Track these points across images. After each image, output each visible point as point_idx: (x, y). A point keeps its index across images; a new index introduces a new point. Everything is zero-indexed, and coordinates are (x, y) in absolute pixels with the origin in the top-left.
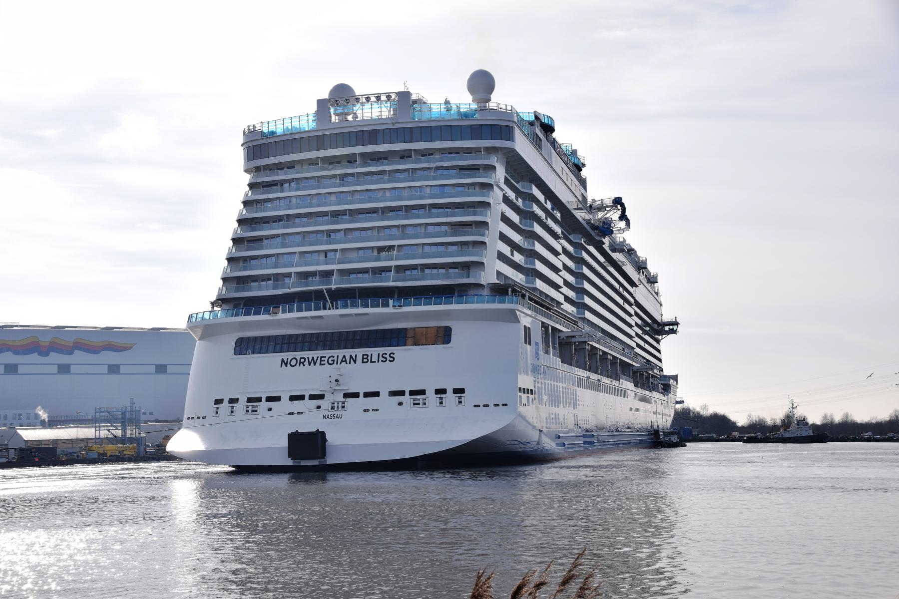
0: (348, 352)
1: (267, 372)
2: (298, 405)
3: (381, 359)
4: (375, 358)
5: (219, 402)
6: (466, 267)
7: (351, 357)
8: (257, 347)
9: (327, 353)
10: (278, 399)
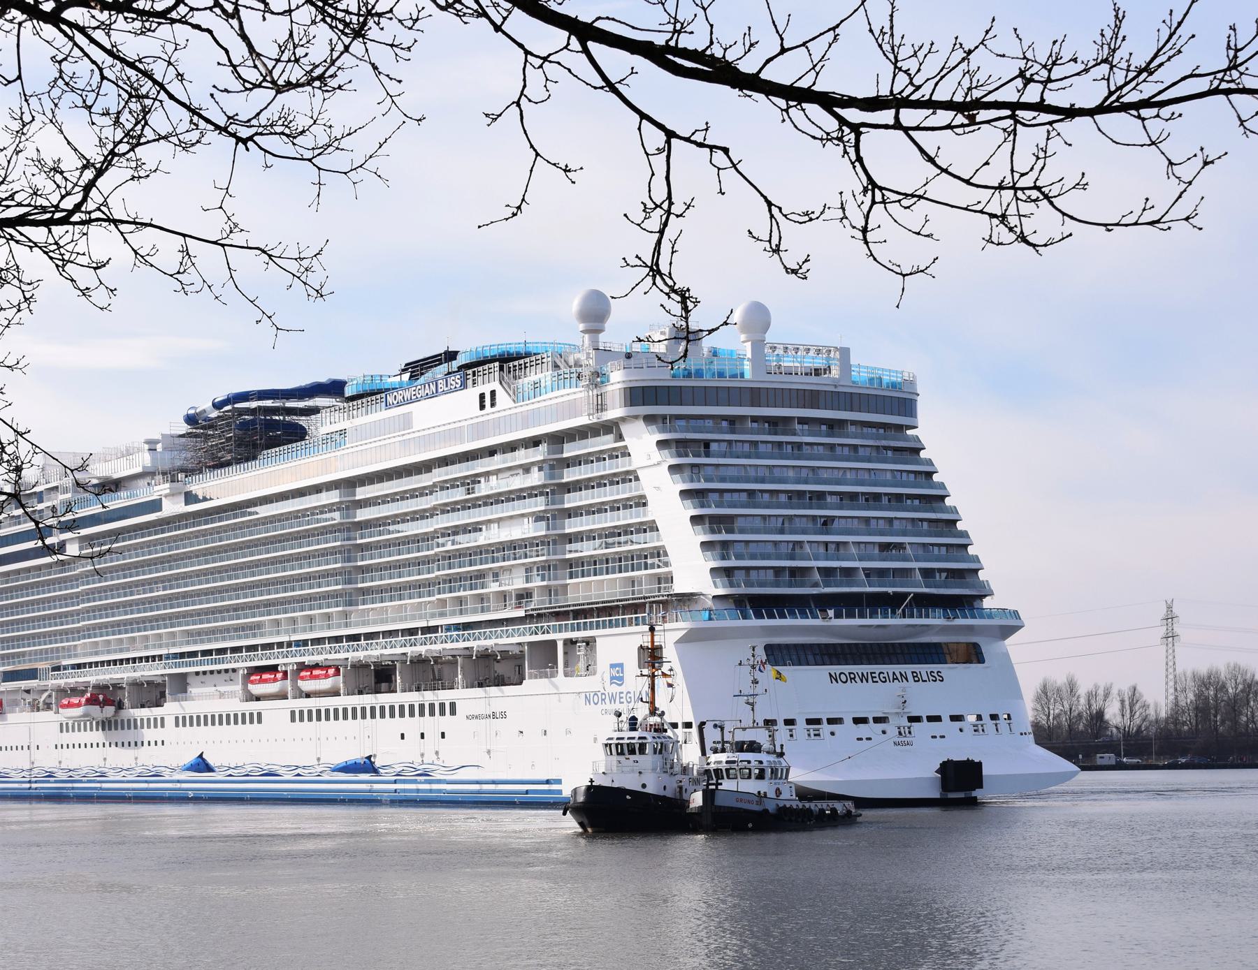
1: (810, 687)
4: (925, 678)
6: (953, 573)
9: (877, 668)
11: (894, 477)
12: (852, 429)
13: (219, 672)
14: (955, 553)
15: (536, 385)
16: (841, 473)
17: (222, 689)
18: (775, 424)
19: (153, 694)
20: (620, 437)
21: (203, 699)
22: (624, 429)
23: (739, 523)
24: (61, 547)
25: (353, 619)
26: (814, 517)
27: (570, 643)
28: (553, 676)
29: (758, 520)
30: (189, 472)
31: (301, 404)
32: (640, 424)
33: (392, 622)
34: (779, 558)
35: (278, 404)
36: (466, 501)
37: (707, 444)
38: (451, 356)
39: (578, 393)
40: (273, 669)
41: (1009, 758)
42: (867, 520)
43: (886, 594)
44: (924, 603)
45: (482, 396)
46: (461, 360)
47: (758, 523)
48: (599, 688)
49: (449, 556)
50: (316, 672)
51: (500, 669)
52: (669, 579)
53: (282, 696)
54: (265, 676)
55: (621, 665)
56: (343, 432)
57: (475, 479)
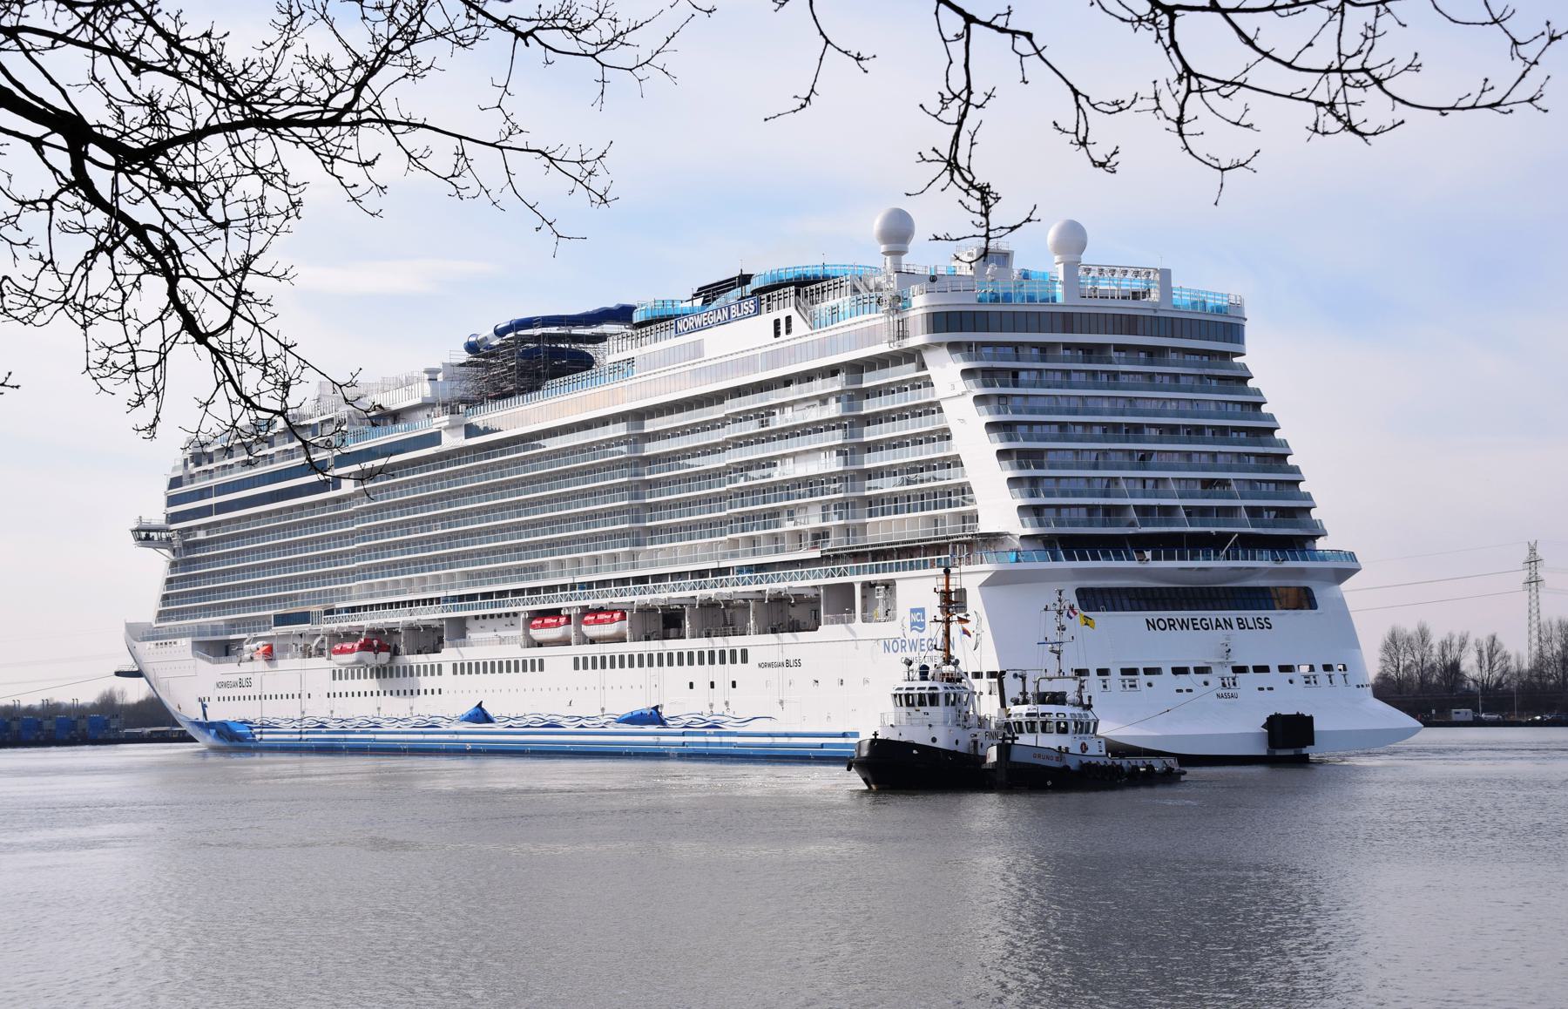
1: (1124, 635)
6: (1281, 512)
11: (1219, 408)
12: (1173, 356)
13: (500, 616)
14: (1285, 490)
15: (834, 311)
16: (1162, 404)
17: (502, 634)
18: (1090, 351)
19: (430, 639)
20: (923, 366)
21: (483, 645)
22: (928, 357)
23: (1049, 457)
24: (336, 482)
25: (640, 560)
26: (1131, 452)
27: (869, 587)
28: (851, 621)
29: (1070, 455)
30: (471, 403)
31: (588, 331)
32: (945, 351)
33: (680, 563)
34: (1092, 495)
35: (563, 331)
36: (760, 434)
37: (1015, 373)
38: (745, 279)
39: (878, 319)
40: (556, 613)
41: (1344, 713)
42: (1189, 454)
43: (1209, 534)
44: (1250, 544)
45: (777, 323)
46: (756, 284)
47: (1070, 457)
48: (898, 634)
49: (742, 493)
50: (601, 617)
51: (795, 613)
52: (974, 517)
53: (566, 642)
54: (547, 621)
55: (922, 610)
56: (631, 361)
57: (769, 411)
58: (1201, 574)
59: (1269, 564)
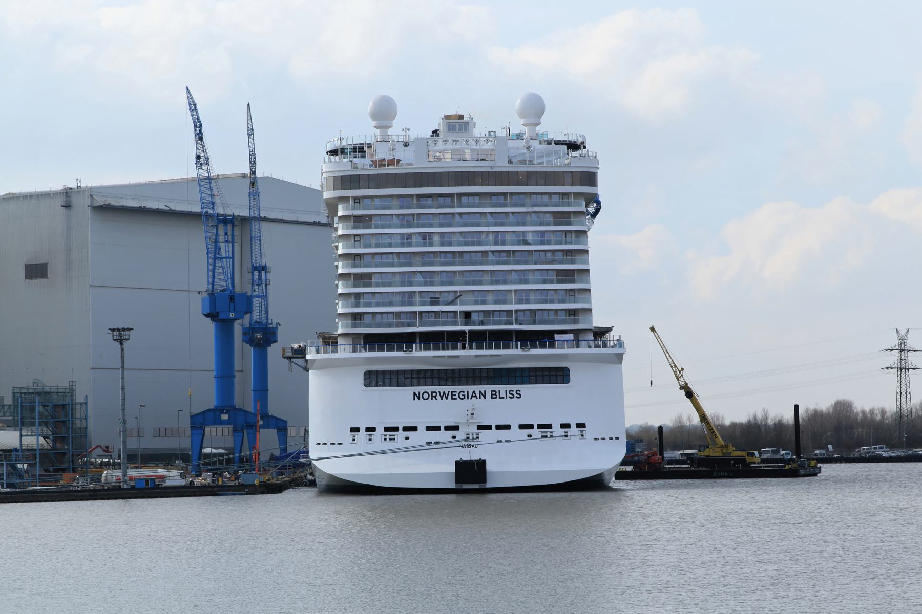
0: (477, 388)
1: (399, 404)
2: (434, 436)
3: (509, 395)
4: (503, 395)
5: (355, 430)
6: (573, 313)
7: (480, 392)
8: (387, 381)
9: (458, 388)
10: (414, 429)
58: (451, 360)
59: (519, 351)
